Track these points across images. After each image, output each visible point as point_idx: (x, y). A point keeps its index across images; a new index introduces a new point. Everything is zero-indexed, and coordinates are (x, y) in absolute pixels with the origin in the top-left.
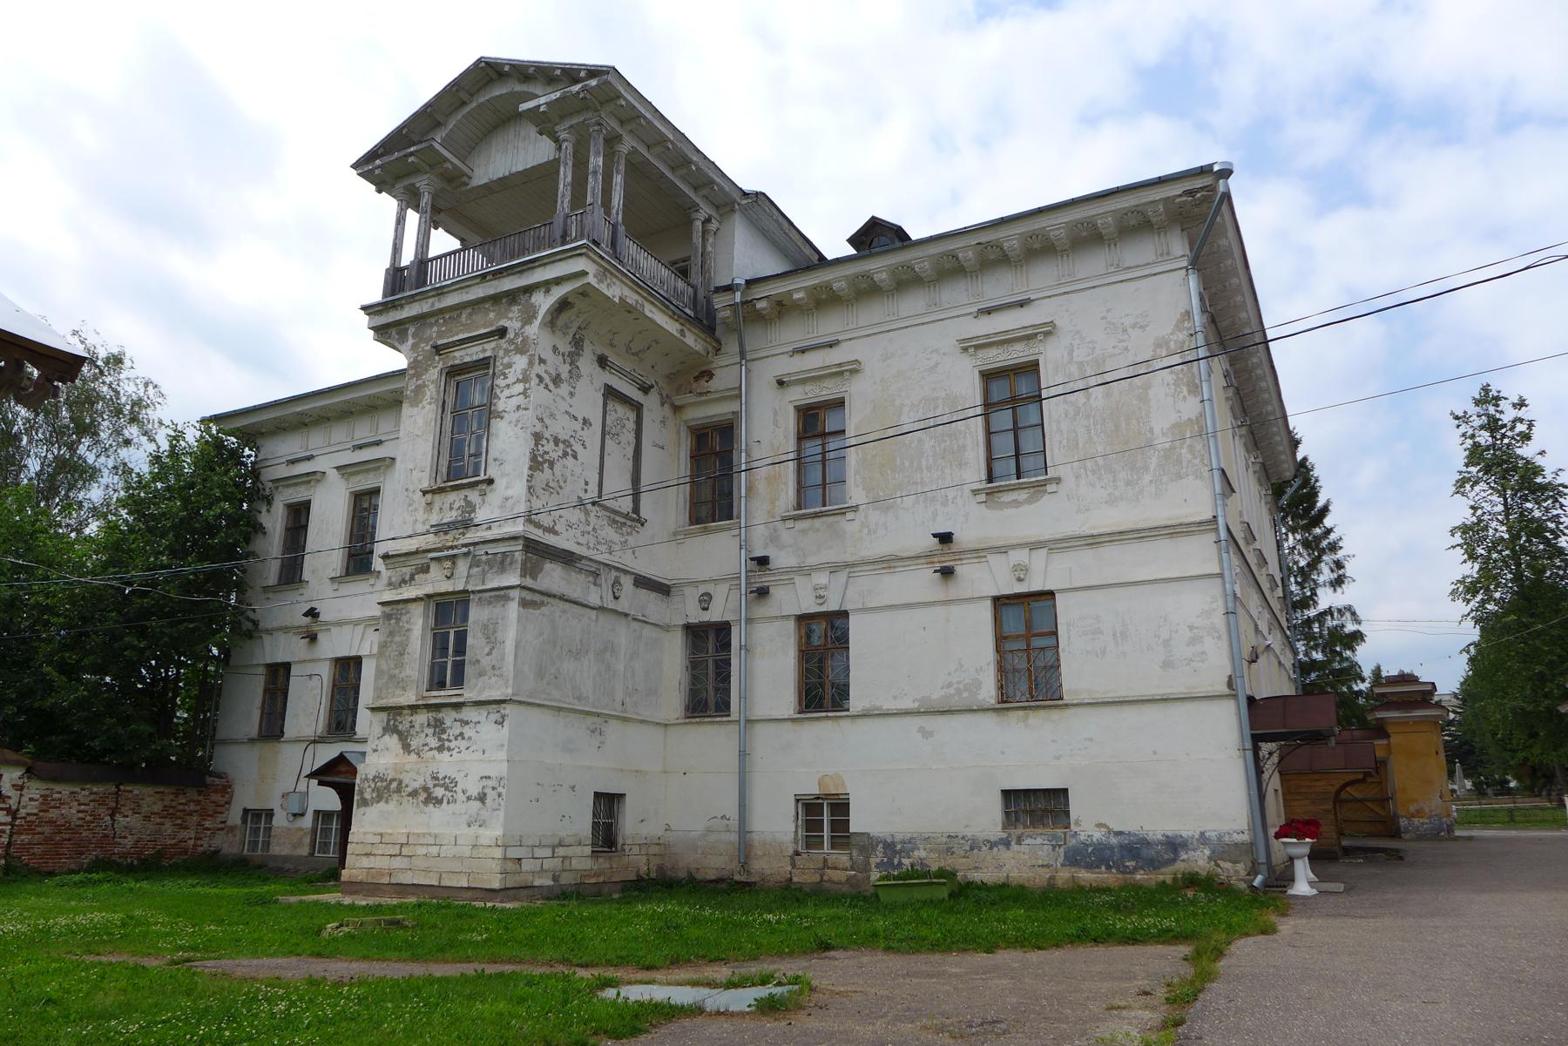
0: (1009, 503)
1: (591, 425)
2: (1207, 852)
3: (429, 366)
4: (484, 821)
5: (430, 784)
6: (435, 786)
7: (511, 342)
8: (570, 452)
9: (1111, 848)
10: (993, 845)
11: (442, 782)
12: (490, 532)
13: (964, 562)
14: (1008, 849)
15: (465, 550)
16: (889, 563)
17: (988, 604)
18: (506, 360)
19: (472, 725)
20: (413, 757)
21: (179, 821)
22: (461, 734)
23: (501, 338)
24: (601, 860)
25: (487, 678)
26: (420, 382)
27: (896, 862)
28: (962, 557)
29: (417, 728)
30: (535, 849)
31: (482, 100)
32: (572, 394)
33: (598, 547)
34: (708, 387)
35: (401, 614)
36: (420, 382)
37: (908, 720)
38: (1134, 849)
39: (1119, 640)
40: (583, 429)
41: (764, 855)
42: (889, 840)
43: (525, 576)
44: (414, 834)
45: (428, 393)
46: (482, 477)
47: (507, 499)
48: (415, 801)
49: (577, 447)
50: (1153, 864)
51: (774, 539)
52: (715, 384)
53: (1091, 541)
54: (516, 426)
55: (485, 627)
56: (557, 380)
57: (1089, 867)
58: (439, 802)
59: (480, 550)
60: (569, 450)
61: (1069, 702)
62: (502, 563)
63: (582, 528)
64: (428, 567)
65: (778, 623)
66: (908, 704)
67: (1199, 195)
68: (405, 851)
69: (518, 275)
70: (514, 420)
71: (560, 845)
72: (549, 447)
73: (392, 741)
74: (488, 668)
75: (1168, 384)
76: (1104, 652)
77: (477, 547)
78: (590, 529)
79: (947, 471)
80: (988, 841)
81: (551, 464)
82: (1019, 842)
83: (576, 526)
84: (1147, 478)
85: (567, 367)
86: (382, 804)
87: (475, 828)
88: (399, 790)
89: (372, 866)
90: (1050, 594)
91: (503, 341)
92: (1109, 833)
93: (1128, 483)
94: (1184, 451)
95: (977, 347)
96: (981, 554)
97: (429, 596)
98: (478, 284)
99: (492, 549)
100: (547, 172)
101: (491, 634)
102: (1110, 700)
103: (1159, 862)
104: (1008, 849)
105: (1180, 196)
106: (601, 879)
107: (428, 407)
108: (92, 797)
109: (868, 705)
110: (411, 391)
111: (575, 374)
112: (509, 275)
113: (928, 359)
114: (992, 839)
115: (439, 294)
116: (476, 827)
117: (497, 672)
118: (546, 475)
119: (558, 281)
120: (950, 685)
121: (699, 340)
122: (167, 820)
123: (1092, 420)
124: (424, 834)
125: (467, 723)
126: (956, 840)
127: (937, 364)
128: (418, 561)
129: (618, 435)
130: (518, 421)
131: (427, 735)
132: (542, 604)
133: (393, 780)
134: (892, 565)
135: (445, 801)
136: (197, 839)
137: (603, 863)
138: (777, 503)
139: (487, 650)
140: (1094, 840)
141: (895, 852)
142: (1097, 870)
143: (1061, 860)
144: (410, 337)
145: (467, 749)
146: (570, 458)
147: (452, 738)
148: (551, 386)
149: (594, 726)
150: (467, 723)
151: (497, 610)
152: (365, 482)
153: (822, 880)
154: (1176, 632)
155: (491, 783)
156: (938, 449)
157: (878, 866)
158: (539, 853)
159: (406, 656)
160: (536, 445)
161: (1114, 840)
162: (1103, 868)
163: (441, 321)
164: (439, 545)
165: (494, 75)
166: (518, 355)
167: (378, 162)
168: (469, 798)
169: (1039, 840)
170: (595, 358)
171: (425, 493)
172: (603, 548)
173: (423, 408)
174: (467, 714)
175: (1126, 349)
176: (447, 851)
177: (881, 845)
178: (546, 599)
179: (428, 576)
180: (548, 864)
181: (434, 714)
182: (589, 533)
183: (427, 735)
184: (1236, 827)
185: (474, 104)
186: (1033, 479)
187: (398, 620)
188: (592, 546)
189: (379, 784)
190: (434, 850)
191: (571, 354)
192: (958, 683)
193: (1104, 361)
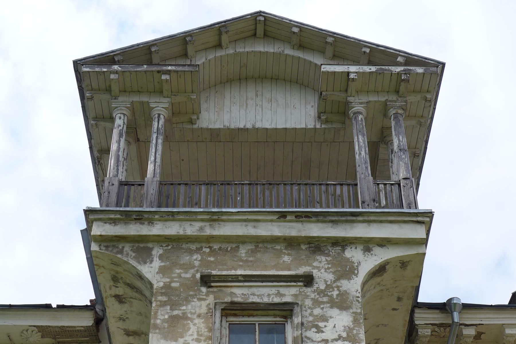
3: (193, 296)
7: (320, 292)
18: (317, 311)
23: (305, 286)
31: (240, 50)
45: (193, 329)
69: (330, 224)
91: (309, 289)
98: (272, 221)
110: (164, 321)
112: (318, 221)
115: (214, 220)
163: (208, 250)
167: (116, 67)
185: (231, 51)
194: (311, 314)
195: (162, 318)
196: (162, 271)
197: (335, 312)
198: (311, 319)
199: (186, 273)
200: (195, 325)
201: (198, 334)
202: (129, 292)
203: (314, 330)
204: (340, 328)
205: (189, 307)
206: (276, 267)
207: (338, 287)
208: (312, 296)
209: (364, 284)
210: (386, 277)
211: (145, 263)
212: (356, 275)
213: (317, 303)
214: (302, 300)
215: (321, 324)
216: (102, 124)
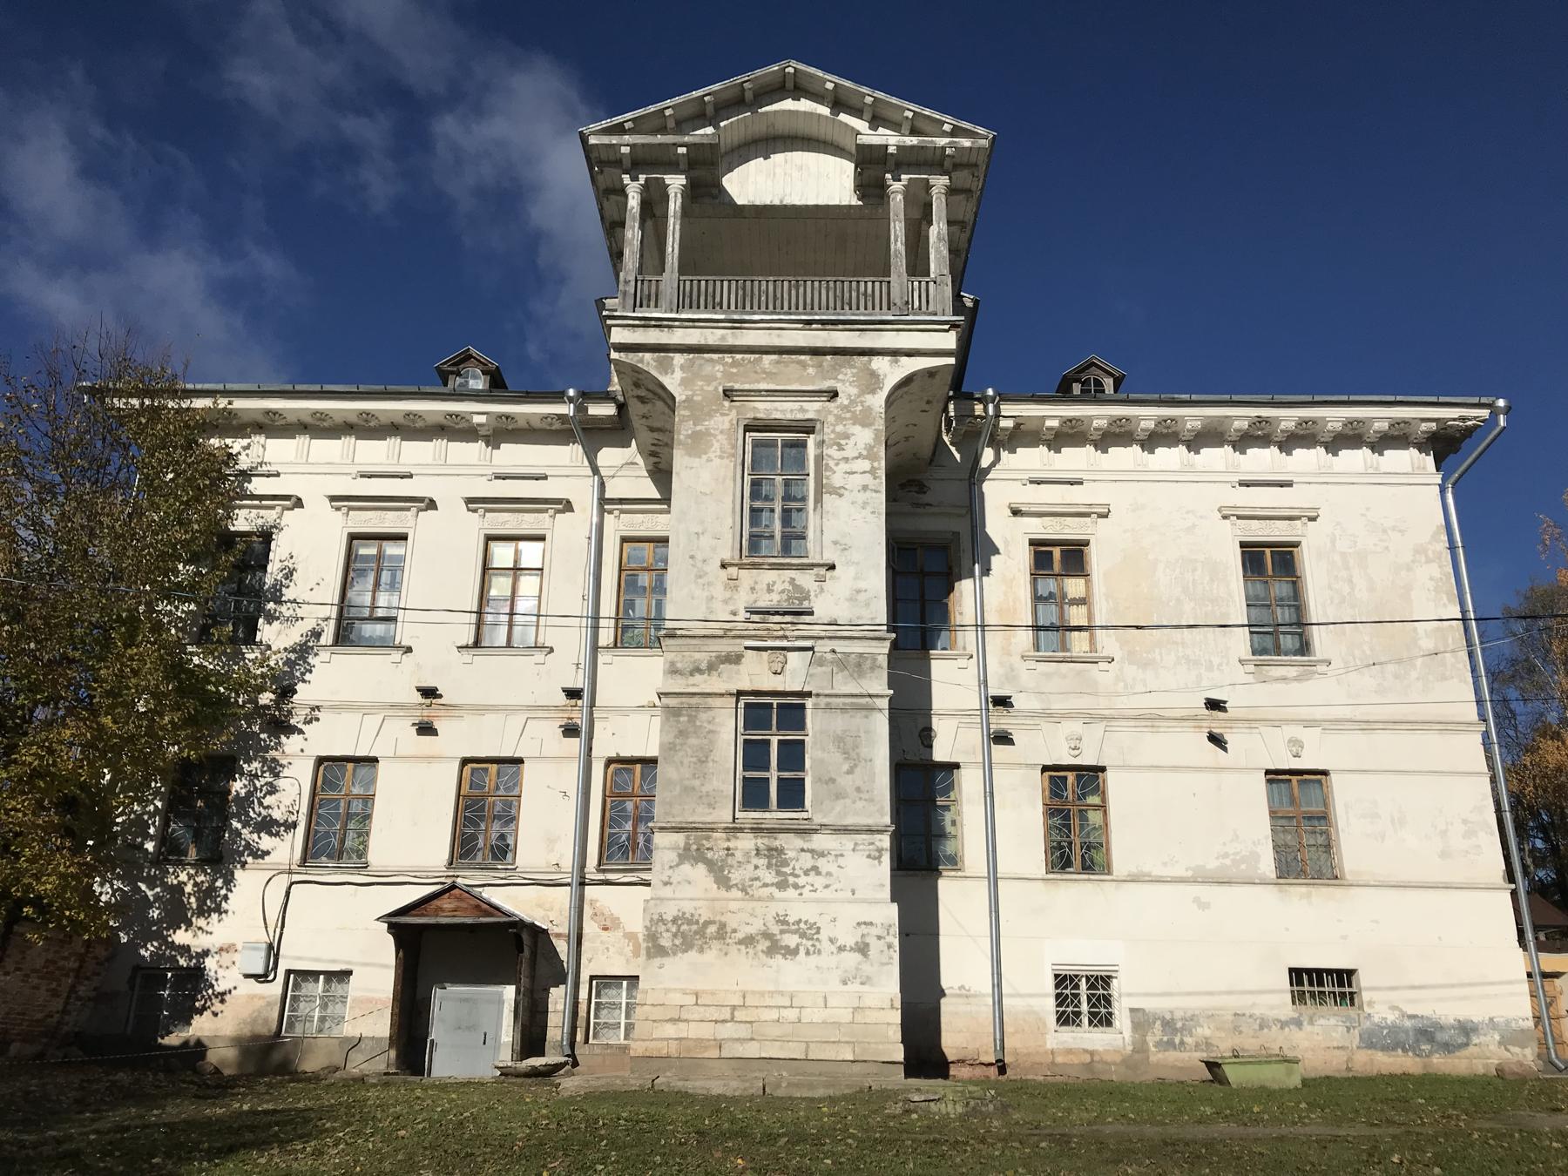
2: (1497, 1037)
3: (716, 411)
5: (775, 929)
6: (782, 932)
7: (845, 408)
9: (1406, 1032)
10: (1283, 1024)
13: (1234, 730)
14: (1301, 1029)
16: (1151, 720)
18: (839, 428)
19: (831, 858)
25: (848, 801)
27: (1177, 1041)
29: (739, 856)
37: (1181, 887)
38: (1427, 1034)
41: (1016, 1032)
42: (1168, 1017)
44: (753, 992)
45: (716, 445)
47: (859, 591)
48: (751, 951)
50: (1448, 1048)
51: (1011, 675)
53: (1365, 727)
57: (1384, 1048)
58: (792, 952)
59: (822, 647)
66: (1179, 871)
68: (739, 1015)
70: (860, 502)
77: (820, 642)
80: (1280, 1021)
82: (1311, 1022)
84: (1414, 674)
87: (854, 987)
92: (1403, 1016)
95: (1239, 517)
96: (1253, 726)
97: (740, 694)
99: (841, 646)
103: (1453, 1045)
104: (1301, 1029)
105: (1454, 420)
107: (717, 461)
110: (688, 436)
114: (1283, 1018)
119: (910, 353)
120: (1226, 855)
124: (773, 992)
125: (822, 854)
127: (1194, 526)
128: (725, 646)
131: (756, 867)
133: (708, 923)
134: (1157, 724)
135: (802, 951)
139: (846, 767)
140: (1389, 1022)
141: (1175, 1031)
142: (1393, 1053)
143: (1356, 1041)
144: (677, 370)
150: (822, 854)
151: (858, 720)
153: (1092, 1061)
155: (874, 931)
157: (1158, 1044)
159: (711, 764)
161: (1408, 1023)
162: (1400, 1051)
163: (730, 360)
168: (841, 949)
169: (1333, 1021)
173: (710, 460)
174: (820, 841)
175: (1387, 548)
176: (814, 1015)
177: (1158, 1022)
181: (766, 841)
183: (756, 867)
184: (1521, 1014)
189: (685, 927)
190: (791, 1014)
194: (833, 431)
195: (685, 433)
196: (684, 383)
197: (857, 429)
198: (832, 436)
199: (708, 385)
200: (718, 441)
201: (722, 452)
202: (650, 395)
203: (835, 447)
204: (861, 446)
205: (712, 422)
206: (800, 380)
207: (862, 402)
208: (836, 412)
209: (889, 401)
210: (914, 387)
211: (666, 374)
212: (881, 389)
213: (839, 419)
214: (826, 417)
215: (843, 442)
216: (613, 198)
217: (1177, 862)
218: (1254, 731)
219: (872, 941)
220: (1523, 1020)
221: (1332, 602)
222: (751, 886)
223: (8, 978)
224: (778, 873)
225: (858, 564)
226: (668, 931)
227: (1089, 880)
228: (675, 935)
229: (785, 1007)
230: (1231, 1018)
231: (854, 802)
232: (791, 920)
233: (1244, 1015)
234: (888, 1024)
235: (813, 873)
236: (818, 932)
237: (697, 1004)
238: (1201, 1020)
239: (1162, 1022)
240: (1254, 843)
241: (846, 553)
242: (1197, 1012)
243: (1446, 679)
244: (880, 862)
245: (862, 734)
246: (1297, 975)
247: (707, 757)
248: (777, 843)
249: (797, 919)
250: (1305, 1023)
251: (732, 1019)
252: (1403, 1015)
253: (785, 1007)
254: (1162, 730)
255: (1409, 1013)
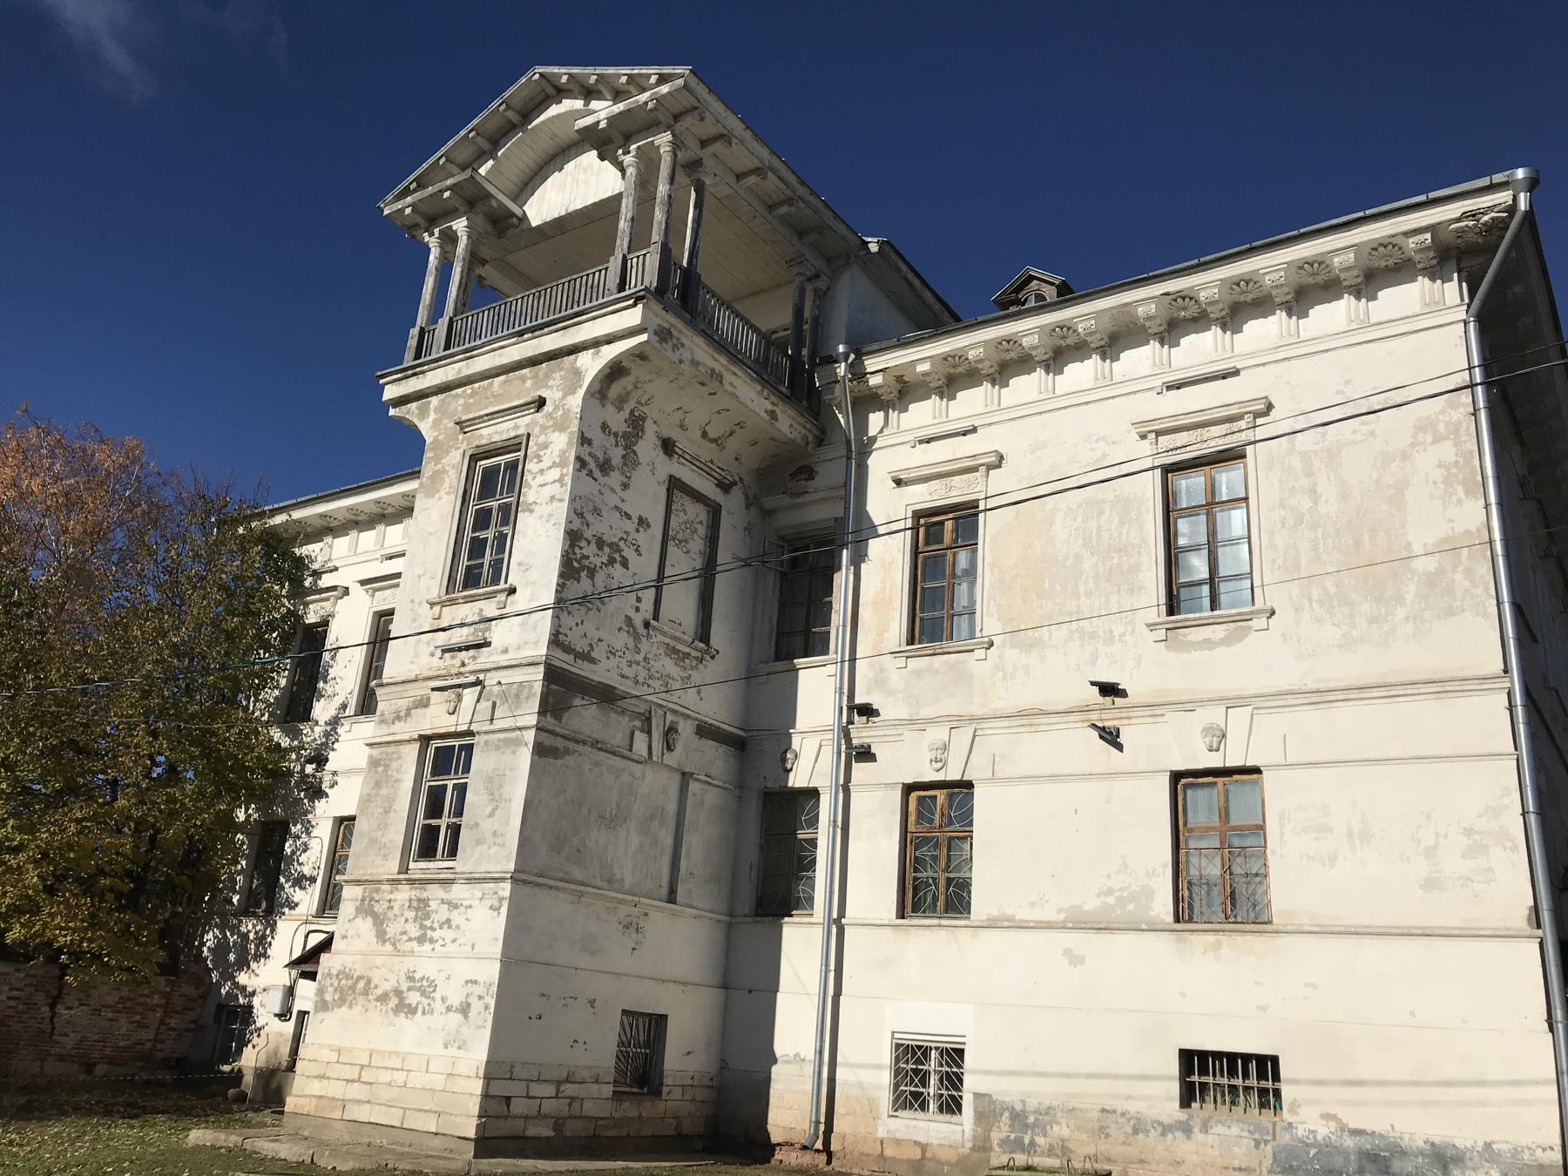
0: (1198, 643)
1: (649, 526)
3: (451, 447)
4: (465, 1042)
5: (404, 987)
6: (409, 989)
7: (550, 415)
8: (618, 559)
9: (1345, 1154)
10: (1166, 1129)
11: (418, 985)
12: (506, 657)
13: (1133, 721)
14: (1189, 1138)
15: (472, 679)
17: (1165, 782)
18: (542, 439)
19: (462, 909)
20: (388, 947)
21: (138, 1018)
22: (448, 921)
24: (626, 1105)
25: (485, 847)
26: (439, 467)
27: (1027, 1141)
28: (1131, 714)
29: (396, 910)
30: (531, 1084)
32: (625, 486)
33: (650, 682)
34: (806, 487)
35: (391, 760)
36: (439, 467)
39: (1357, 841)
40: (638, 531)
41: (848, 1114)
42: (1018, 1107)
43: (545, 716)
45: (447, 481)
46: (502, 586)
48: (384, 1008)
49: (629, 553)
51: (880, 681)
52: (818, 482)
54: (548, 521)
55: (490, 779)
56: (605, 467)
60: (617, 556)
61: (1281, 928)
62: (517, 696)
63: (629, 656)
64: (429, 699)
65: (880, 794)
66: (1050, 914)
67: (1486, 218)
68: (366, 1076)
71: (568, 1080)
72: (590, 550)
73: (365, 926)
74: (488, 835)
75: (1435, 483)
76: (1333, 859)
77: (489, 675)
78: (640, 658)
79: (1114, 598)
80: (1161, 1124)
81: (592, 573)
82: (1205, 1129)
83: (621, 654)
84: (1401, 613)
85: (620, 452)
86: (344, 1008)
87: (453, 1051)
88: (366, 992)
89: (323, 1093)
90: (1256, 770)
92: (1342, 1130)
93: (1373, 620)
94: (1458, 576)
95: (1159, 433)
96: (1158, 712)
100: (606, 210)
101: (495, 785)
102: (1342, 929)
104: (1189, 1138)
105: (1458, 220)
106: (624, 1132)
107: (445, 498)
108: (28, 981)
109: (996, 913)
111: (631, 460)
113: (1093, 450)
114: (1166, 1120)
116: (455, 1049)
117: (498, 840)
118: (584, 586)
119: (610, 339)
120: (1109, 892)
121: (796, 425)
122: (123, 1015)
123: (1320, 530)
124: (390, 1053)
126: (1113, 1117)
128: (421, 690)
129: (686, 541)
130: (550, 515)
131: (407, 920)
132: (567, 752)
133: (360, 978)
136: (156, 1040)
137: (629, 1109)
138: (886, 635)
139: (489, 810)
140: (1319, 1138)
141: (1026, 1126)
144: (432, 413)
145: (454, 941)
146: (617, 565)
147: (436, 925)
148: (597, 474)
149: (628, 919)
150: (456, 907)
152: (384, 600)
153: (923, 1157)
154: (1446, 837)
155: (478, 990)
156: (1101, 571)
158: (536, 1090)
159: (392, 814)
160: (572, 546)
161: (1349, 1142)
164: (444, 672)
165: (550, 91)
166: (557, 434)
168: (449, 1009)
169: (1235, 1130)
170: (659, 443)
171: (432, 604)
172: (657, 684)
173: (440, 499)
174: (459, 891)
175: (1372, 433)
176: (417, 1080)
177: (1006, 1114)
178: (571, 745)
179: (428, 710)
180: (548, 1106)
182: (638, 663)
186: (1234, 611)
187: (387, 767)
188: (641, 680)
190: (399, 1077)
191: (626, 436)
192: (1119, 890)
193: (1340, 452)
217: (1047, 902)
218: (1160, 719)
219: (473, 1000)
220: (1544, 1150)
221: (1283, 525)
222: (399, 940)
223: (72, 1012)
224: (422, 927)
225: (534, 583)
226: (332, 985)
227: (940, 926)
228: (335, 990)
229: (397, 1069)
230: (1096, 1115)
231: (489, 847)
232: (417, 976)
233: (1114, 1112)
234: (471, 1094)
235: (446, 926)
236: (434, 991)
237: (338, 1062)
238: (1059, 1115)
239: (1011, 1114)
240: (1147, 874)
241: (527, 573)
242: (1055, 1104)
243: (1453, 614)
244: (499, 913)
245: (508, 773)
246: (1192, 1061)
247: (390, 807)
248: (425, 895)
249: (421, 976)
250: (1196, 1130)
251: (359, 1080)
252: (1343, 1128)
253: (397, 1069)
254: (1042, 728)
255: (1353, 1125)
